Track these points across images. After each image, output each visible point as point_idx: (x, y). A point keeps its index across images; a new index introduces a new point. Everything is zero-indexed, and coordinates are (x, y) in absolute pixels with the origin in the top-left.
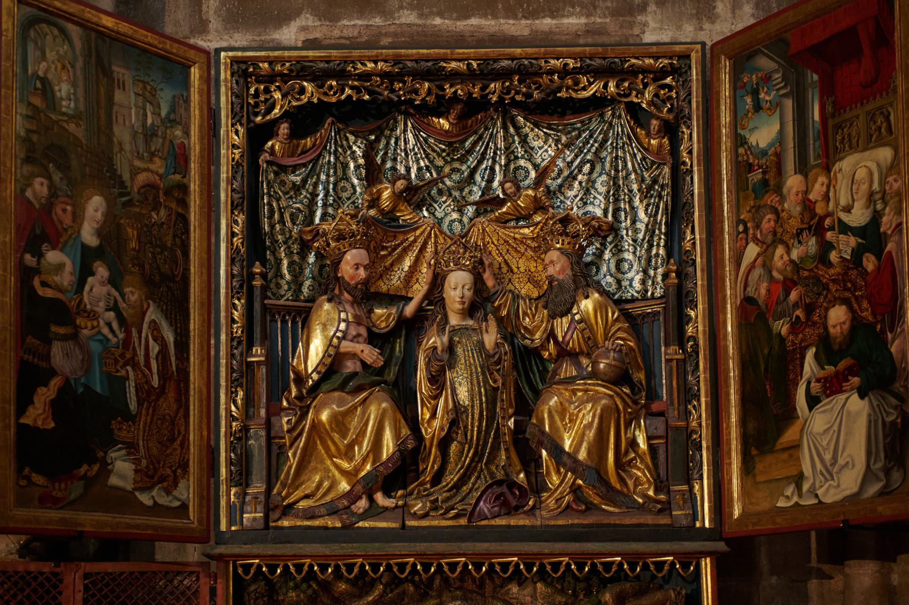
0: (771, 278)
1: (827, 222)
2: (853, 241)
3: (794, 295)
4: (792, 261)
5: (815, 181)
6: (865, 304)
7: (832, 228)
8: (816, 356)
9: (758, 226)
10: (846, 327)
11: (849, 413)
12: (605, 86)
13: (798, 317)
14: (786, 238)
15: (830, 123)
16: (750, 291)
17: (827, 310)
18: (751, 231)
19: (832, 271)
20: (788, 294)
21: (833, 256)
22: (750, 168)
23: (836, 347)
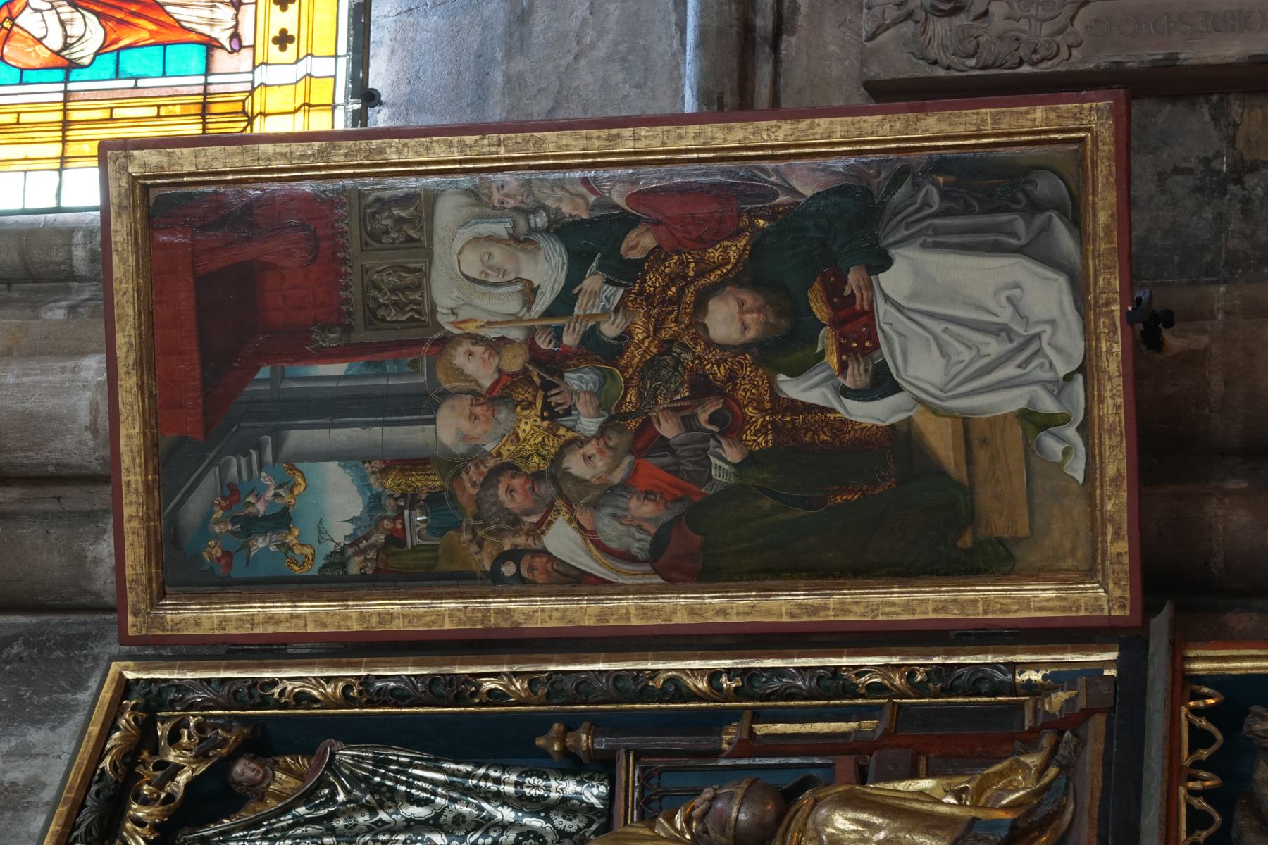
0: (625, 487)
1: (543, 343)
2: (593, 282)
3: (668, 429)
4: (602, 432)
5: (459, 372)
6: (715, 254)
7: (558, 333)
8: (795, 372)
9: (514, 521)
10: (749, 298)
11: (914, 295)
12: (140, 823)
13: (712, 420)
14: (553, 446)
15: (362, 336)
16: (639, 544)
17: (710, 345)
18: (521, 541)
19: (639, 334)
20: (663, 444)
21: (610, 329)
22: (395, 540)
23: (784, 323)
